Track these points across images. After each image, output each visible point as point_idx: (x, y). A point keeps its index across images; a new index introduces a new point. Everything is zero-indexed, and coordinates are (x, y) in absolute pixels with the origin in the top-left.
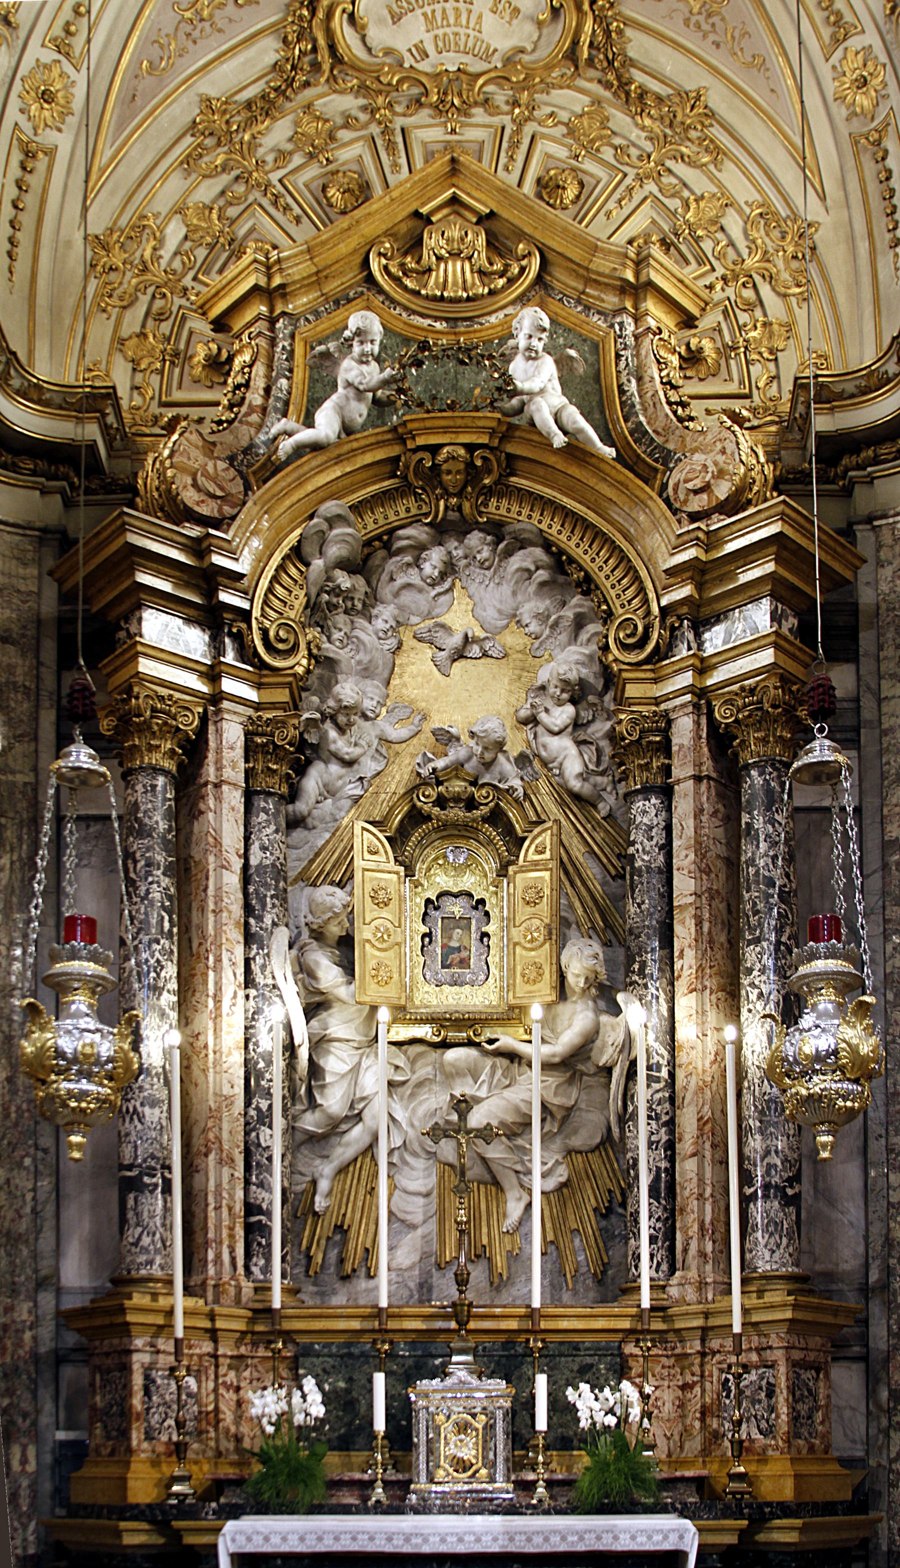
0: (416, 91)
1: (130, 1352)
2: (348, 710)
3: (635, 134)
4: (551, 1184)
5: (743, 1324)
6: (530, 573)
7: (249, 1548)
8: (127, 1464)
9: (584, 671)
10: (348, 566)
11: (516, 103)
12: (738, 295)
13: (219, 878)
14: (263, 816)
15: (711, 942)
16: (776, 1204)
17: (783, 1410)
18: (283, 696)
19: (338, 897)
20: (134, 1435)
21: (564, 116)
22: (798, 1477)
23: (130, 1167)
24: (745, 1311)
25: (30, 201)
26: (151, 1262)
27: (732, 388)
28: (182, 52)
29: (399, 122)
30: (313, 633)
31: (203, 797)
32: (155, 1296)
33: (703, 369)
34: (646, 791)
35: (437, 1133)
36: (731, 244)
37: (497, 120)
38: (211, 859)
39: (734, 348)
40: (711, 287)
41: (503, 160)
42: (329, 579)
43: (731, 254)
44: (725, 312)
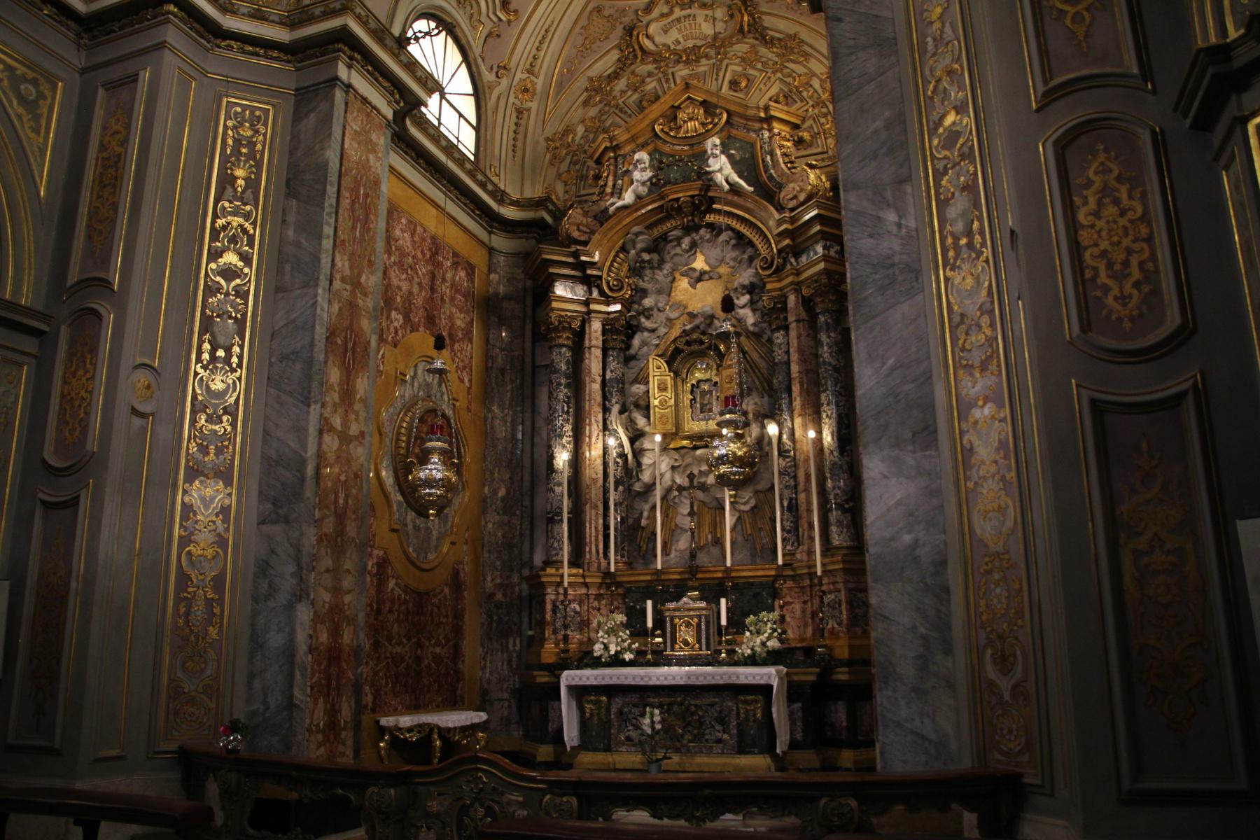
0: (677, 57)
1: (545, 595)
3: (770, 56)
5: (823, 572)
6: (728, 242)
7: (573, 683)
8: (542, 646)
9: (752, 279)
11: (719, 54)
12: (820, 111)
13: (590, 386)
14: (611, 358)
15: (808, 393)
16: (839, 513)
17: (844, 613)
19: (642, 388)
20: (547, 632)
21: (740, 54)
22: (850, 646)
23: (549, 513)
24: (823, 565)
25: (522, 129)
26: (558, 554)
27: (819, 150)
28: (580, 63)
29: (670, 71)
31: (584, 354)
32: (557, 569)
33: (805, 145)
34: (778, 329)
36: (815, 91)
37: (711, 62)
38: (587, 379)
39: (819, 134)
40: (807, 110)
41: (715, 76)
42: (640, 257)
43: (815, 94)
44: (814, 120)
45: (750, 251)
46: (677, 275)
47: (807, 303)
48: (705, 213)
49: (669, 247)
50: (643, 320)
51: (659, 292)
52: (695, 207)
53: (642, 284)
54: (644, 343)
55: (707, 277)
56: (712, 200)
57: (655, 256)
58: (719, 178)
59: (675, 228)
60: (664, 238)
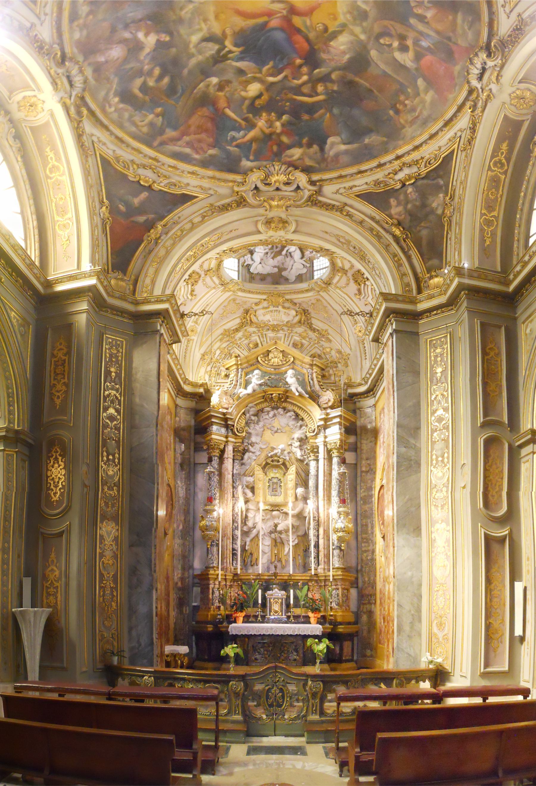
2: (253, 443)
4: (294, 544)
10: (254, 415)
18: (241, 441)
30: (247, 428)
35: (271, 533)
45: (300, 422)
46: (265, 428)
47: (329, 452)
48: (283, 402)
49: (263, 414)
50: (250, 447)
51: (257, 435)
52: (280, 399)
53: (250, 431)
54: (249, 458)
55: (279, 431)
56: (287, 397)
57: (256, 418)
58: (293, 389)
59: (268, 407)
60: (262, 410)
